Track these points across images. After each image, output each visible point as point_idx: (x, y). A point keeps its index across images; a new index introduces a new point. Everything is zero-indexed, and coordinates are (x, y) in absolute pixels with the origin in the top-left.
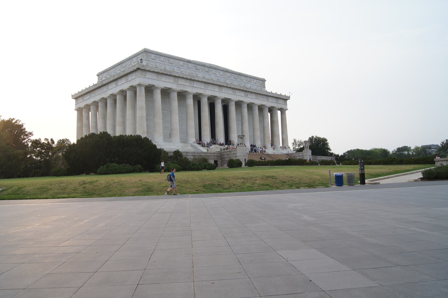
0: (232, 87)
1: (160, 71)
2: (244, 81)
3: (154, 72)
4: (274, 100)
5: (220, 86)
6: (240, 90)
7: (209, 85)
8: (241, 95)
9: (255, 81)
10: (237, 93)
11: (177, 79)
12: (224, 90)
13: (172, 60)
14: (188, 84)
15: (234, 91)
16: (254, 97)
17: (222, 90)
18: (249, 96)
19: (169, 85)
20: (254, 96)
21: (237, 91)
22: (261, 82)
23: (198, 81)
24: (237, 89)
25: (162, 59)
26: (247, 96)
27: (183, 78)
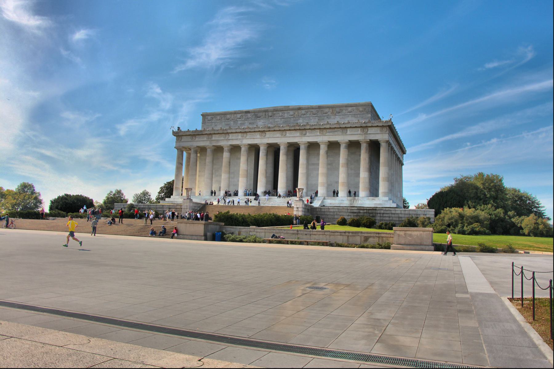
2: (329, 113)
3: (186, 135)
4: (359, 131)
5: (259, 131)
7: (248, 134)
8: (295, 135)
9: (350, 109)
11: (210, 136)
13: (228, 116)
14: (222, 138)
15: (284, 133)
16: (318, 134)
18: (308, 134)
19: (202, 144)
20: (318, 132)
21: (287, 132)
23: (232, 133)
25: (218, 117)
26: (306, 134)
27: (215, 134)
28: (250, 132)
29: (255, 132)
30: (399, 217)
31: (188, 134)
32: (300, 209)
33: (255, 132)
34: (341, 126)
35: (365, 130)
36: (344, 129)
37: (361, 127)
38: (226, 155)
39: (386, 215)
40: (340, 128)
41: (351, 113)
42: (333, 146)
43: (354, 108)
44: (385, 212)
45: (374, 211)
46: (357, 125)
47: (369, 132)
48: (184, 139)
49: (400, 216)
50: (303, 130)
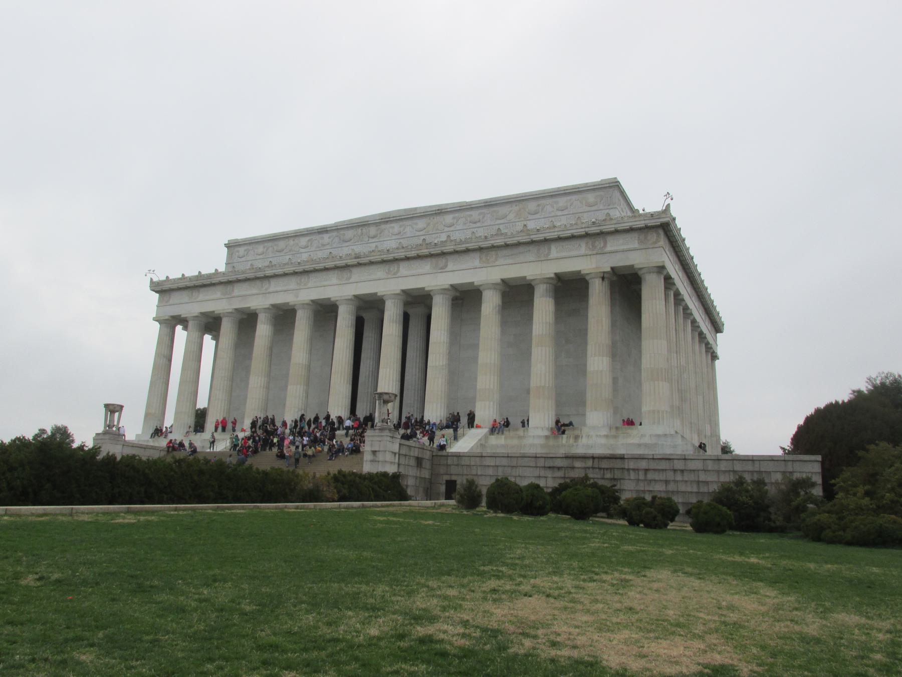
0: (378, 258)
1: (188, 284)
2: (511, 216)
4: (583, 247)
5: (336, 268)
6: (407, 259)
7: (312, 276)
8: (421, 271)
9: (562, 201)
10: (404, 269)
11: (229, 288)
12: (357, 274)
13: (282, 244)
14: (255, 291)
15: (393, 268)
17: (350, 278)
18: (451, 266)
20: (475, 260)
22: (591, 198)
23: (275, 276)
24: (395, 260)
25: (260, 248)
26: (446, 266)
27: (239, 281)
28: (315, 271)
29: (326, 269)
30: (698, 482)
31: (181, 285)
32: (380, 457)
33: (326, 269)
34: (535, 237)
35: (599, 243)
36: (540, 243)
37: (587, 235)
38: (263, 330)
39: (656, 476)
40: (532, 242)
41: (565, 212)
42: (517, 295)
43: (574, 197)
44: (653, 465)
45: (618, 464)
46: (575, 232)
47: (609, 248)
48: (176, 298)
49: (703, 477)
50: (438, 255)
